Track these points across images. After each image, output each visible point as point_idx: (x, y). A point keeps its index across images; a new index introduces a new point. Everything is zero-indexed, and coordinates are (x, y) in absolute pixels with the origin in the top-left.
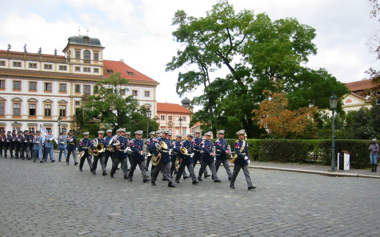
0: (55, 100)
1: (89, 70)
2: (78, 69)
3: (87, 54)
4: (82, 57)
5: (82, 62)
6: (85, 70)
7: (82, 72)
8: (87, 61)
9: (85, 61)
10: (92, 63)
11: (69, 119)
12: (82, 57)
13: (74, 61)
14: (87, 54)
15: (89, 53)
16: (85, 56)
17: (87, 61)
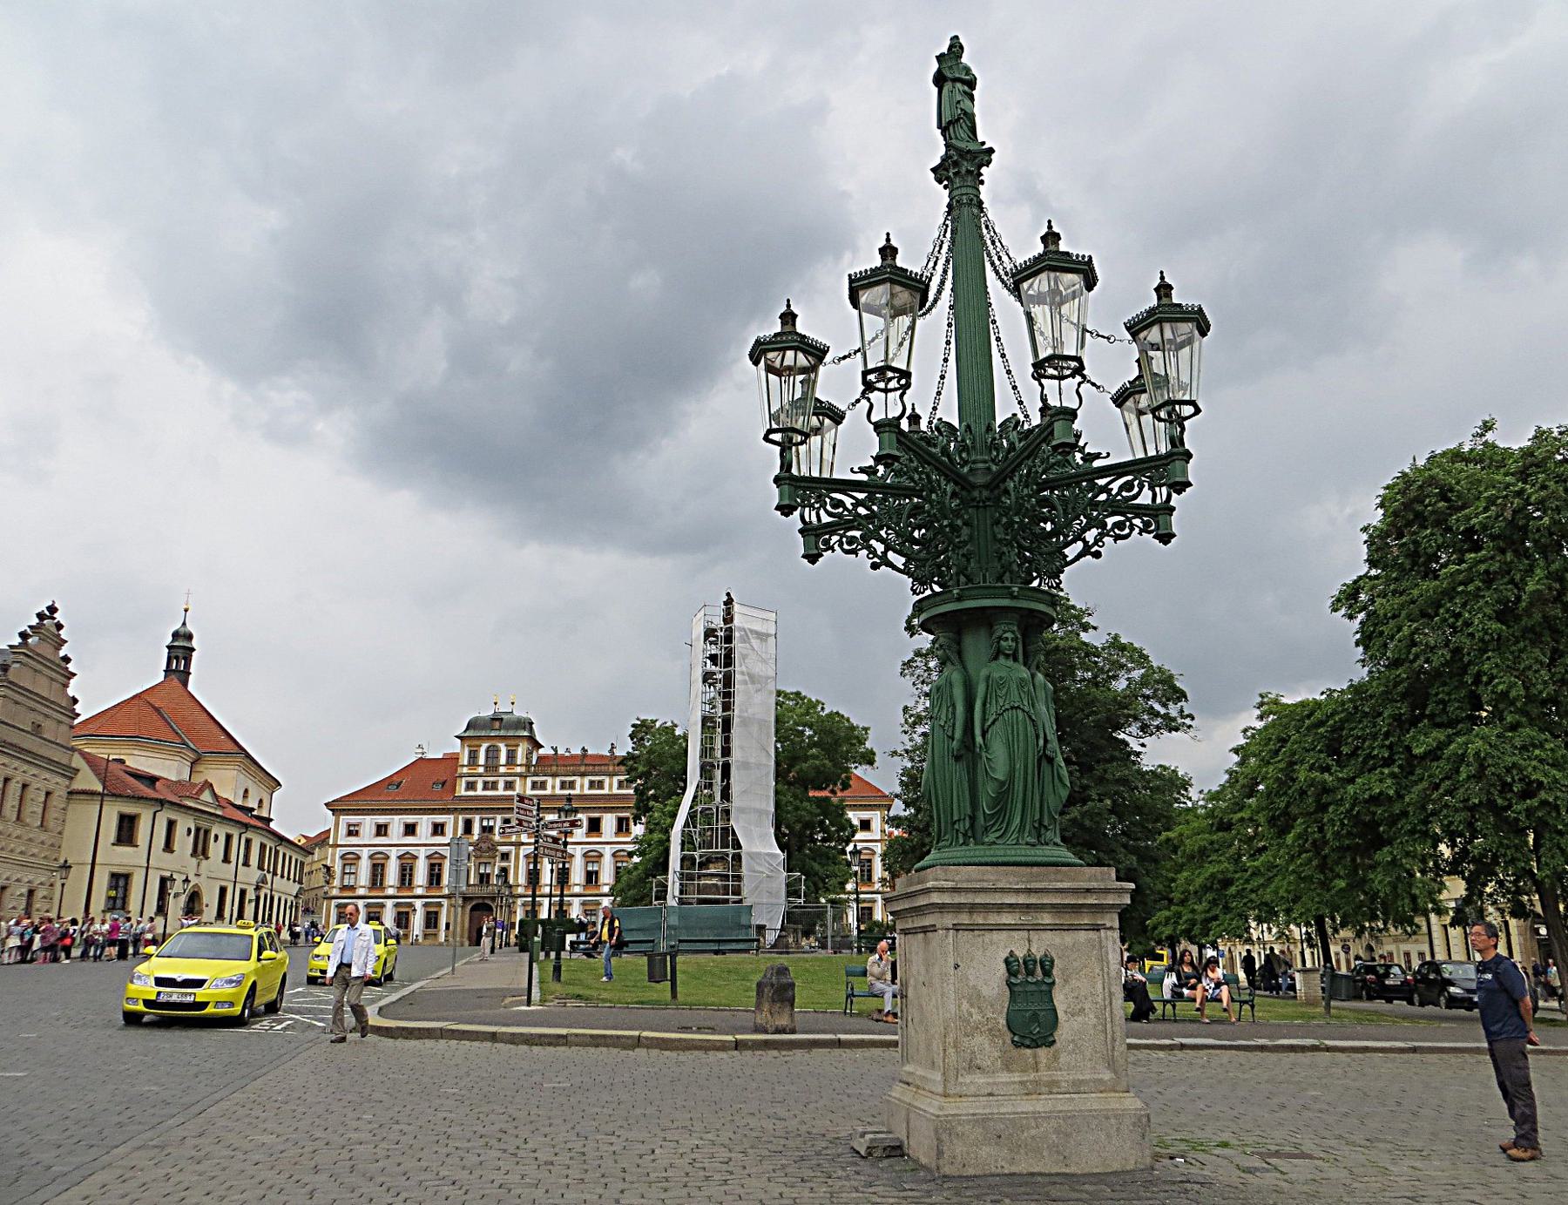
0: (422, 853)
1: (494, 786)
2: (471, 786)
3: (492, 753)
4: (482, 761)
5: (481, 770)
6: (485, 783)
7: (480, 792)
8: (491, 767)
9: (486, 767)
10: (502, 770)
11: (446, 891)
12: (482, 761)
13: (465, 770)
14: (492, 753)
15: (498, 750)
16: (487, 758)
17: (491, 767)
